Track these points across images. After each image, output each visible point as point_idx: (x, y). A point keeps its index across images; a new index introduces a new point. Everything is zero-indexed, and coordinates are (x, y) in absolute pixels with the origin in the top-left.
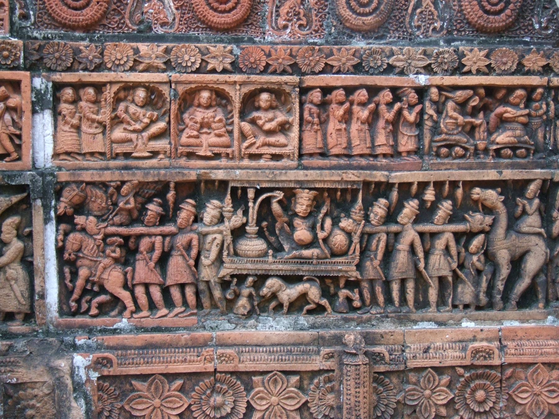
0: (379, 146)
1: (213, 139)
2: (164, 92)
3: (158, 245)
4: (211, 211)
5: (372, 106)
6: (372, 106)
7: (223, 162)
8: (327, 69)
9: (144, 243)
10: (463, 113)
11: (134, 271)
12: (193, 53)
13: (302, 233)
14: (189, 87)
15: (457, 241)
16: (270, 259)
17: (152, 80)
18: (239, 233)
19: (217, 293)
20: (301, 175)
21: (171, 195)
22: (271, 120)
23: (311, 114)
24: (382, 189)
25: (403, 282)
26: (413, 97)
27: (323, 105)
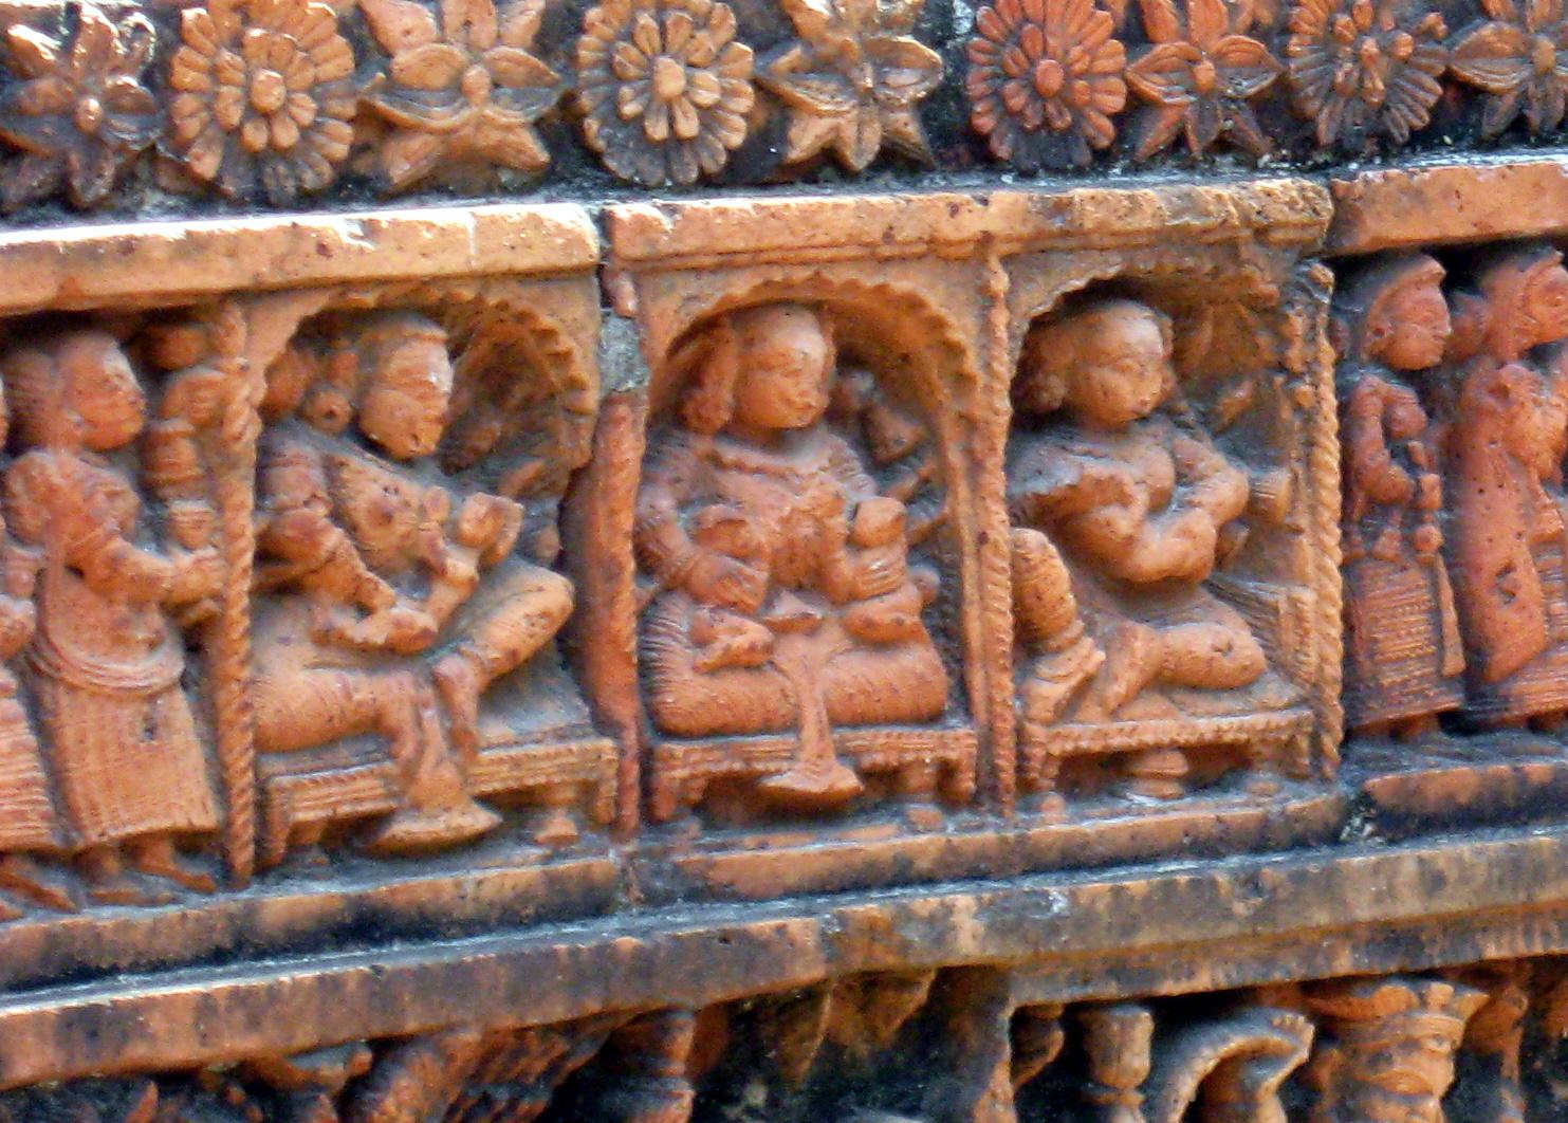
8: (1463, 117)
12: (707, 41)
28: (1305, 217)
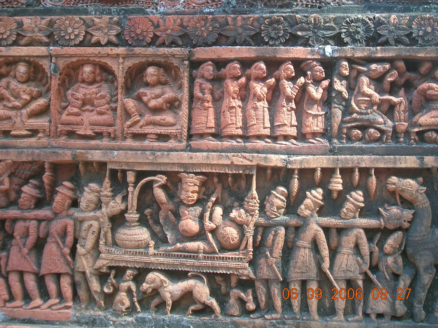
0: (279, 126)
1: (96, 118)
2: (44, 66)
3: (32, 231)
4: (88, 196)
5: (272, 81)
6: (272, 81)
7: (105, 142)
11: (8, 257)
12: (77, 25)
13: (190, 224)
14: (69, 60)
15: (370, 240)
16: (152, 251)
17: (31, 54)
18: (118, 220)
19: (95, 285)
20: (185, 157)
21: (46, 177)
22: (157, 97)
23: (202, 91)
24: (281, 175)
25: (304, 283)
27: (218, 80)
28: (181, 54)
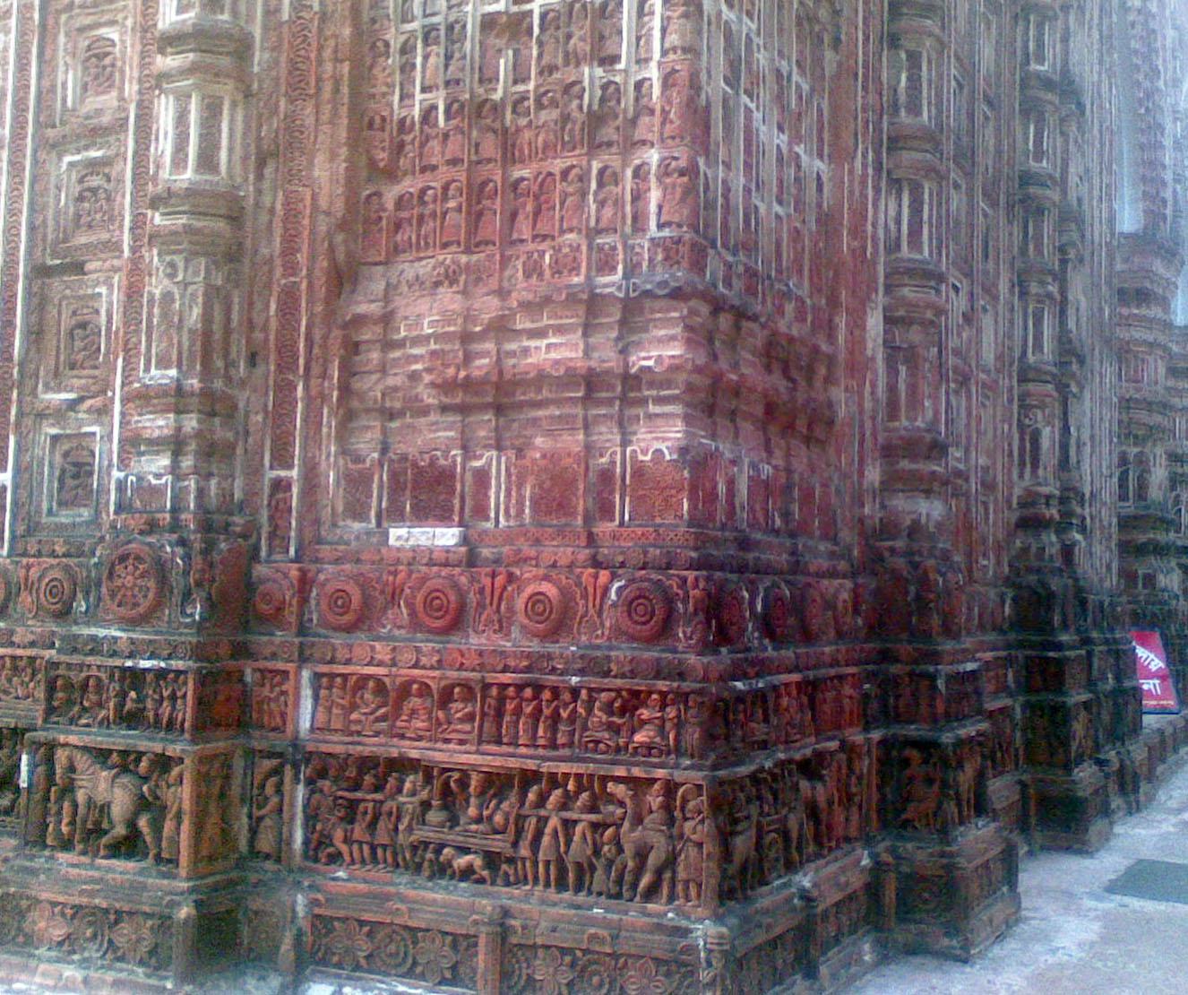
9: (361, 807)
10: (611, 713)
18: (426, 805)
26: (566, 696)
